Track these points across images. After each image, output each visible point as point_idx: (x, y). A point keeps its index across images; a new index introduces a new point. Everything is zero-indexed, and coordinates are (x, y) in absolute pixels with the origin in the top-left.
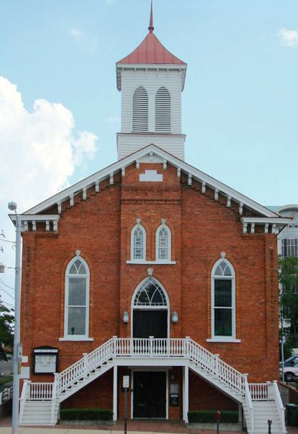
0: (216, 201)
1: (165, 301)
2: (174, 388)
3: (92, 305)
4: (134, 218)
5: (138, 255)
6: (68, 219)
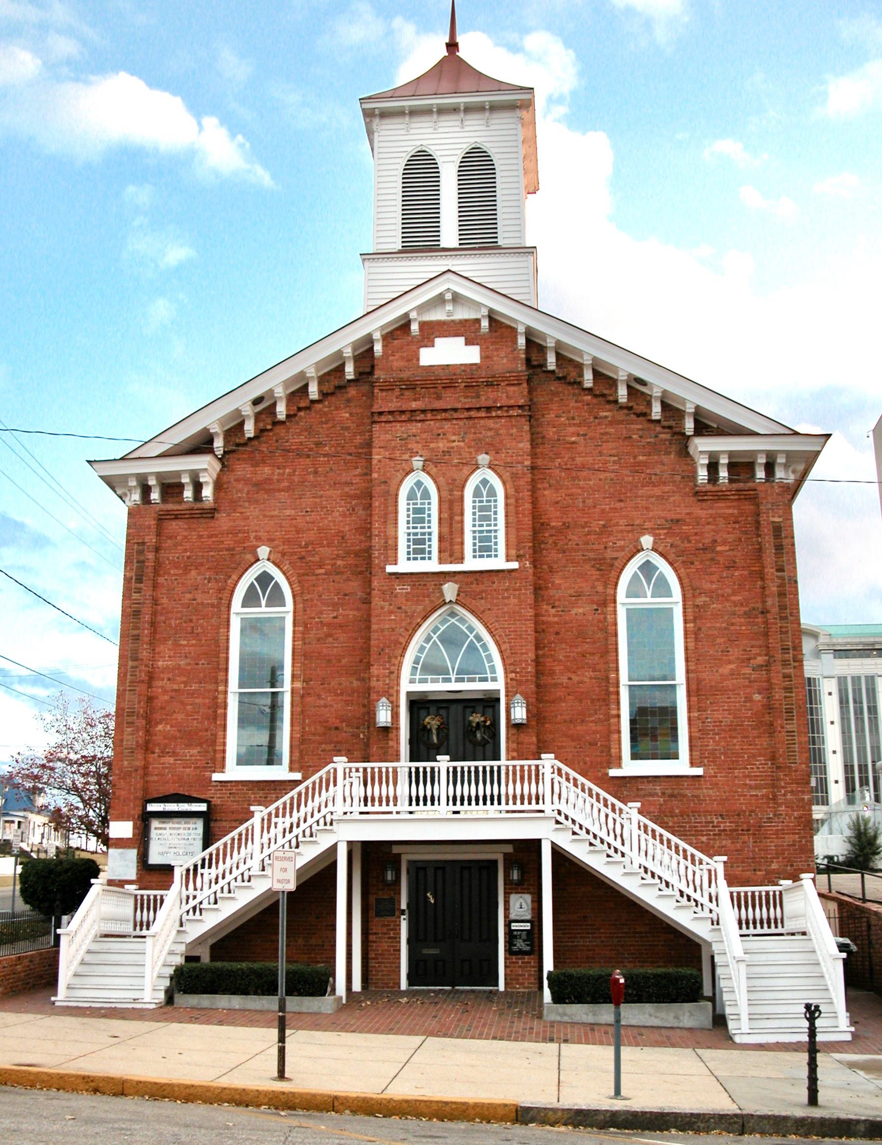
0: (622, 408)
1: (493, 670)
2: (521, 905)
3: (298, 685)
4: (406, 457)
5: (419, 550)
6: (242, 469)
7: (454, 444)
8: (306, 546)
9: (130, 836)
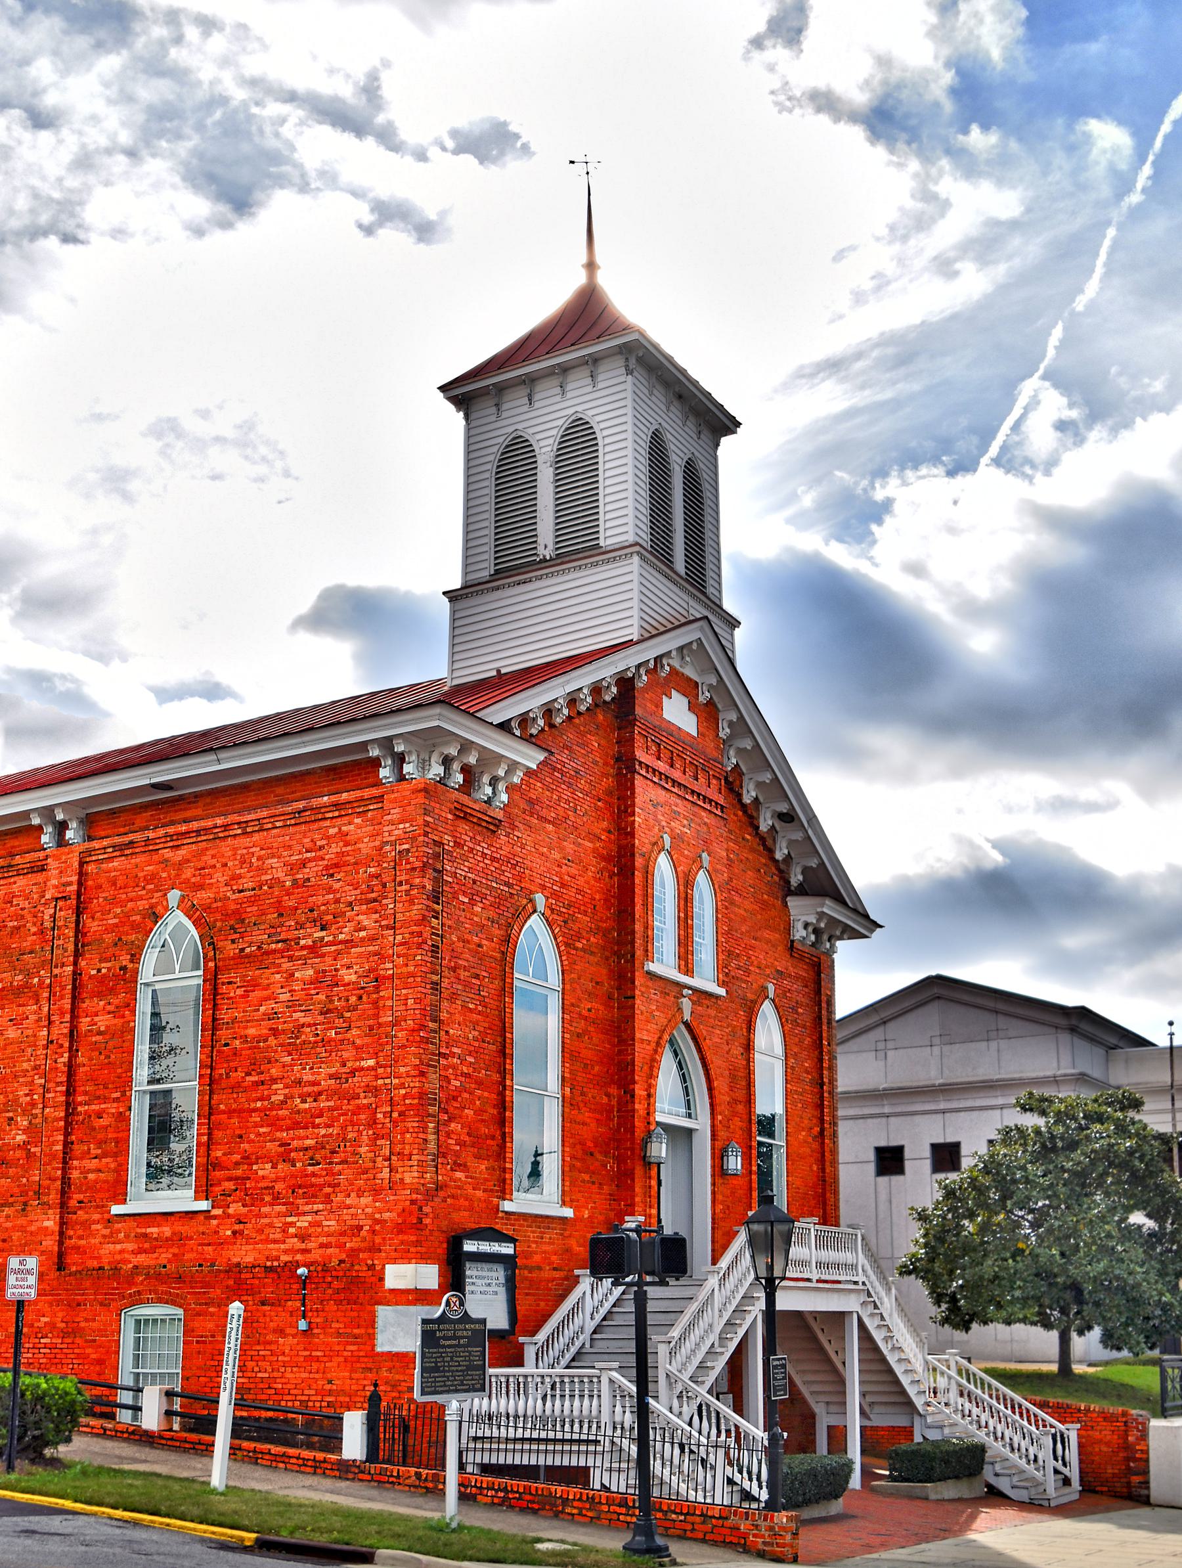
9: (436, 1287)
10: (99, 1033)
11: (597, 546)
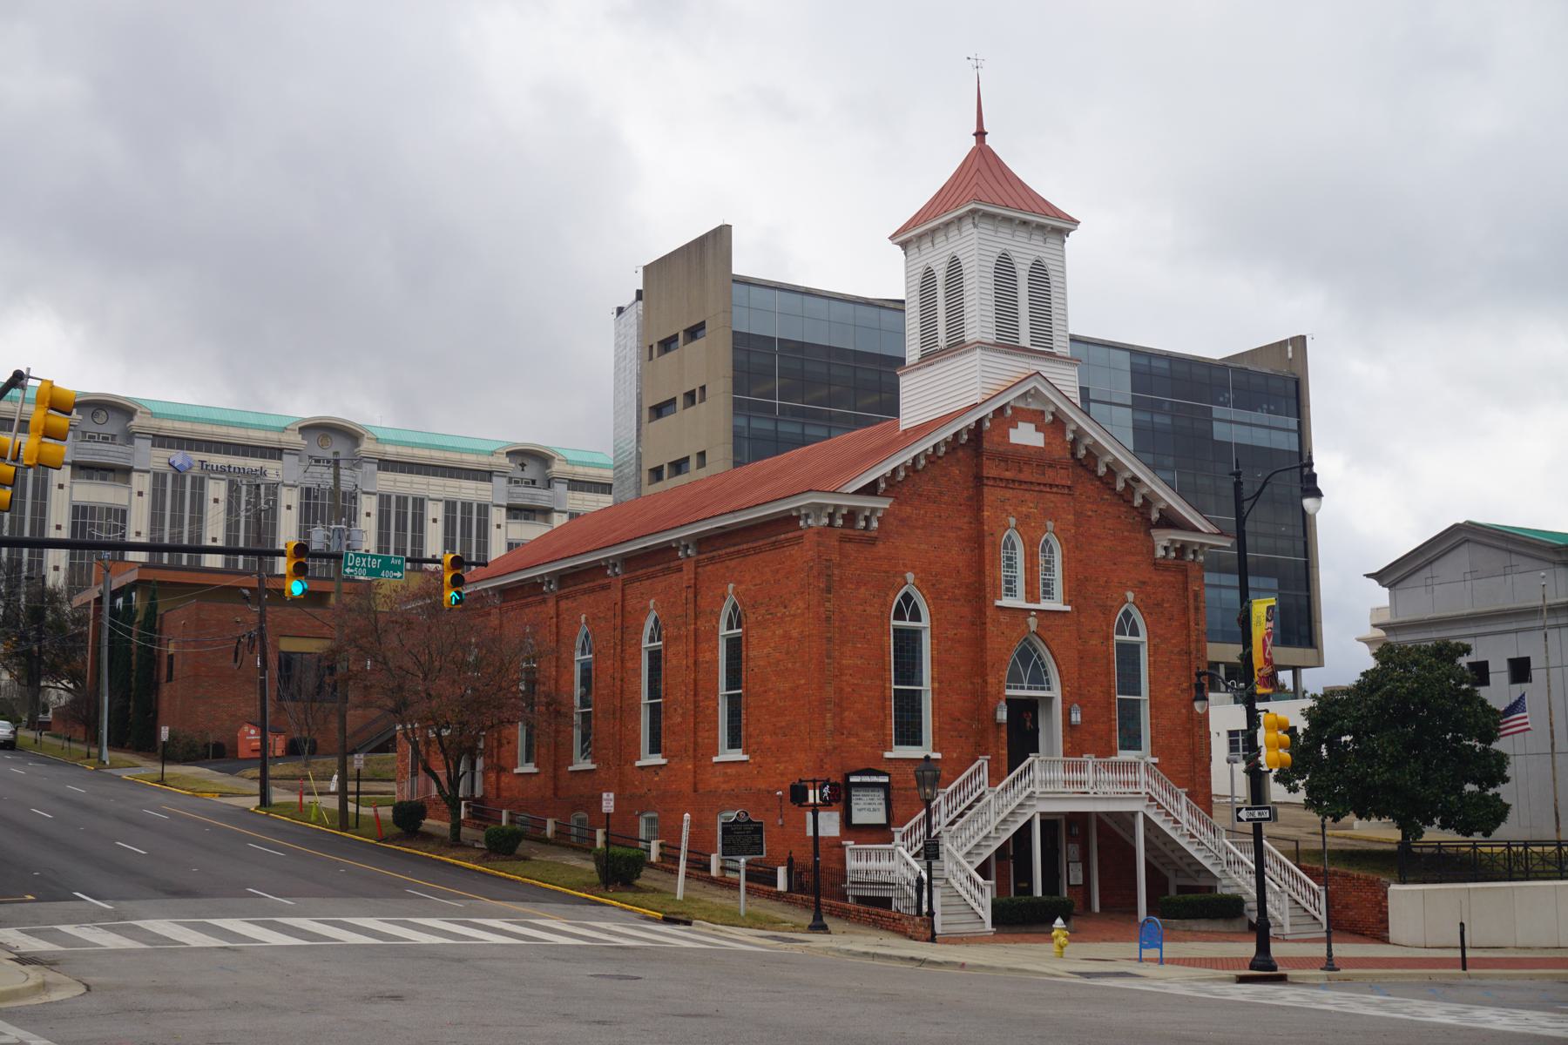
4: (1004, 515)
5: (1011, 591)
7: (1032, 510)
8: (936, 575)
10: (707, 662)
11: (963, 341)
